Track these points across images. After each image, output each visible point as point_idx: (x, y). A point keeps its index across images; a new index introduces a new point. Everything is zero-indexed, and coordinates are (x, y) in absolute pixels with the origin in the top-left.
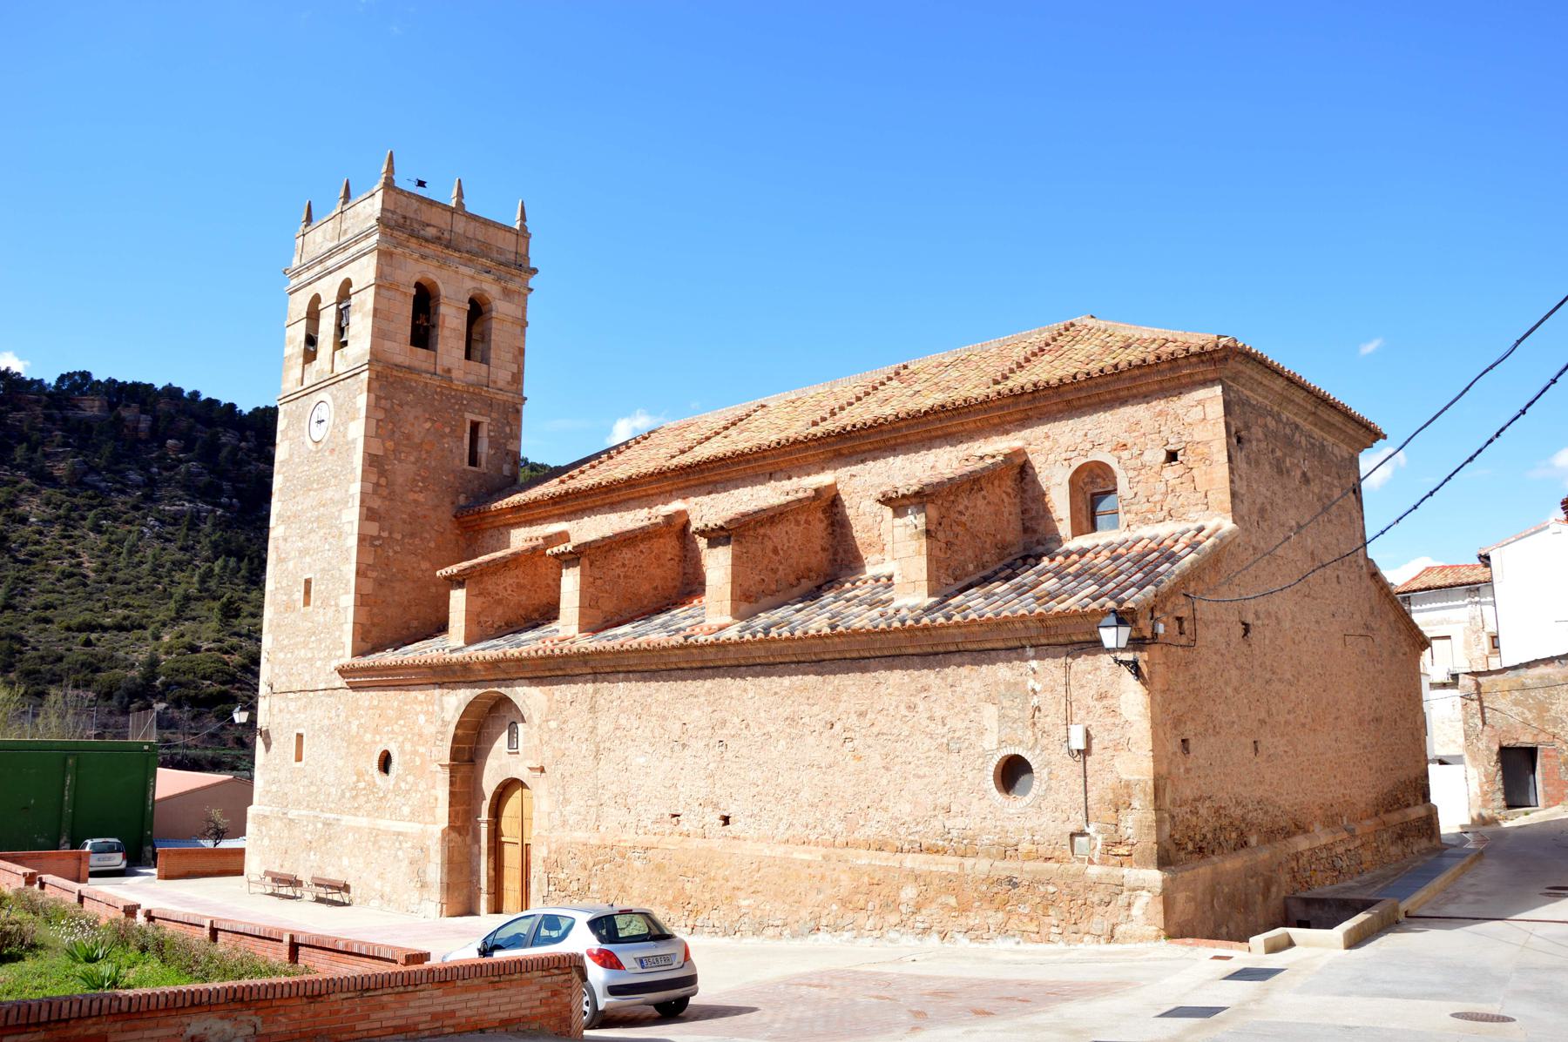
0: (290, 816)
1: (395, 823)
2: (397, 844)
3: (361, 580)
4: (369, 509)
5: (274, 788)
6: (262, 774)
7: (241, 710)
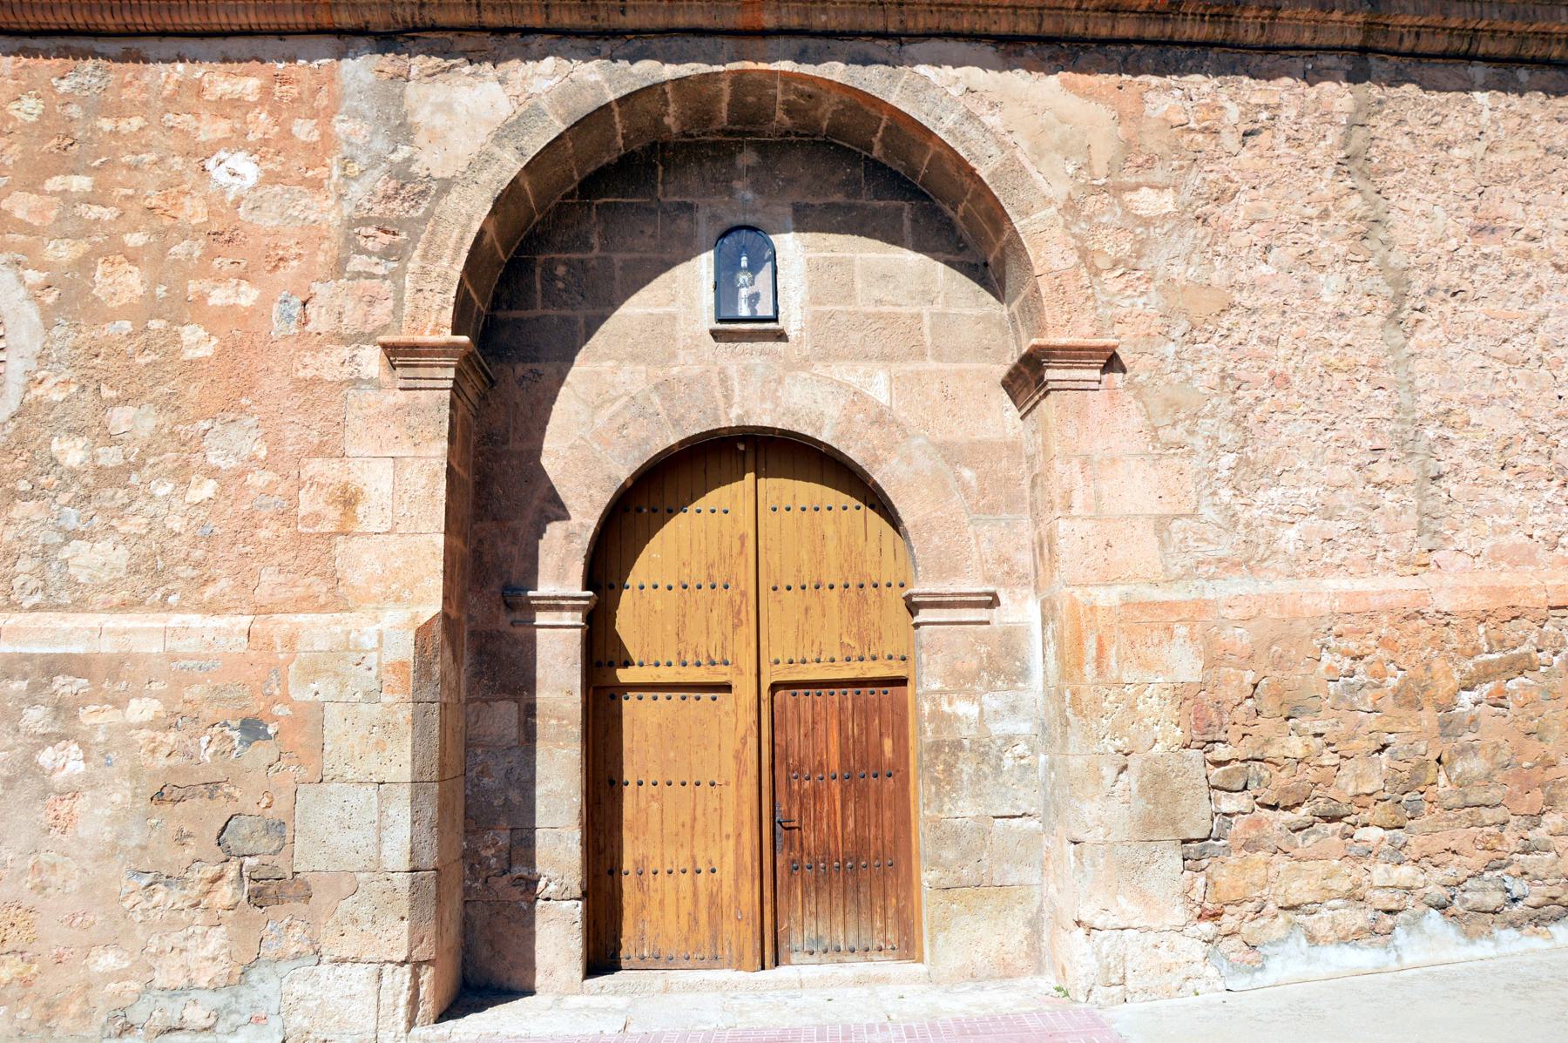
2: (36, 717)
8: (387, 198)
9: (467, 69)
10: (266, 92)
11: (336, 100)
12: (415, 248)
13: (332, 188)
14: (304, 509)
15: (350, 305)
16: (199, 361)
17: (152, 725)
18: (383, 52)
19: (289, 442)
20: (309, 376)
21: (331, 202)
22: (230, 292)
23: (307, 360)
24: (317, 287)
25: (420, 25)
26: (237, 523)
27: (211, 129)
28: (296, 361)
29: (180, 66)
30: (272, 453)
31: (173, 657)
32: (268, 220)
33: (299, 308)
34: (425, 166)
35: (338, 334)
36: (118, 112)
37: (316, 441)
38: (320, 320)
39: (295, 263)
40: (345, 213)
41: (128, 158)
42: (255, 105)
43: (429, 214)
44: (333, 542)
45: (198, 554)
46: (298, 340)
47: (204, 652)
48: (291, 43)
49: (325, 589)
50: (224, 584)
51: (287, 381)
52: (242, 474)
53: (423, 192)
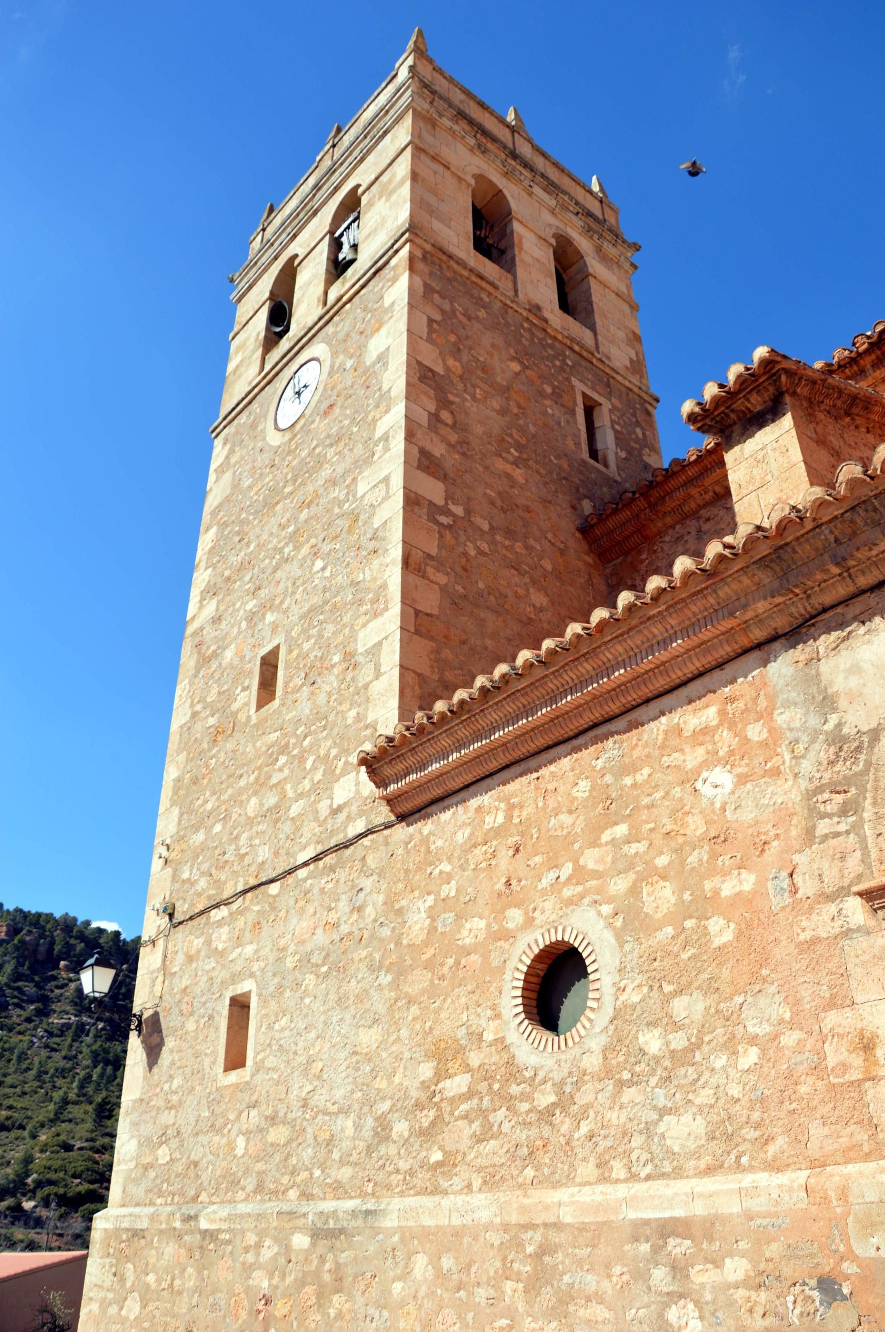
0: (204, 1224)
1: (622, 1191)
2: (660, 1275)
3: (412, 578)
4: (423, 452)
5: (163, 1154)
6: (135, 1124)
7: (98, 963)
8: (832, 763)
9: (862, 630)
10: (722, 713)
11: (772, 699)
12: (865, 798)
13: (788, 771)
14: (831, 1062)
15: (826, 865)
16: (725, 946)
17: (745, 1283)
18: (794, 647)
19: (806, 1000)
20: (808, 937)
21: (790, 783)
22: (735, 882)
23: (804, 924)
24: (796, 858)
25: (814, 613)
26: (780, 1084)
27: (694, 757)
28: (795, 927)
29: (663, 719)
30: (795, 1014)
31: (750, 1216)
32: (747, 815)
33: (787, 880)
34: (853, 725)
35: (823, 894)
36: (633, 769)
37: (827, 995)
38: (807, 887)
39: (775, 843)
40: (803, 788)
41: (646, 801)
42: (718, 726)
43: (868, 764)
44: (863, 1089)
45: (756, 1116)
46: (793, 909)
47: (773, 1209)
48: (729, 669)
49: (866, 1137)
50: (781, 1141)
51: (793, 946)
52: (775, 1037)
53: (858, 747)
